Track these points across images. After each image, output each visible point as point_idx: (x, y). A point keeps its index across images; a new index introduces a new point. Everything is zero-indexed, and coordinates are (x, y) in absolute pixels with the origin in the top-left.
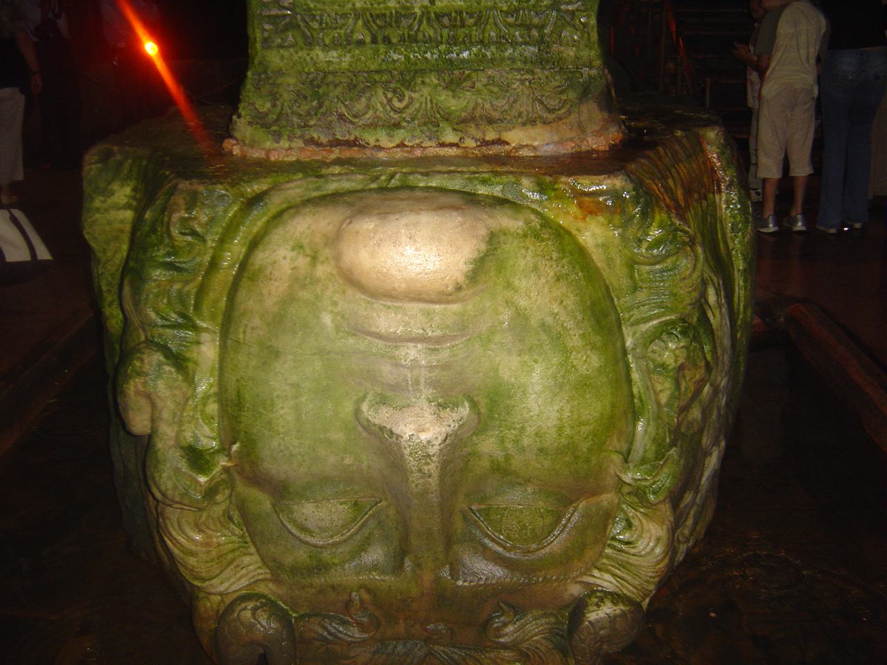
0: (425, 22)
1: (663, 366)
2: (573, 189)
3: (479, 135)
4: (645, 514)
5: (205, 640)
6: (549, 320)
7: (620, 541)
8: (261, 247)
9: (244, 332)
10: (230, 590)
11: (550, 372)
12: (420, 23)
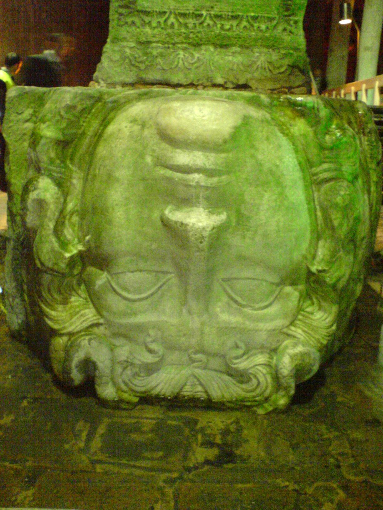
0: (208, 18)
1: (337, 205)
2: (288, 100)
3: (234, 81)
4: (321, 296)
5: (57, 366)
6: (274, 169)
7: (306, 312)
8: (112, 123)
9: (99, 169)
10: (75, 331)
11: (274, 197)
12: (205, 19)
